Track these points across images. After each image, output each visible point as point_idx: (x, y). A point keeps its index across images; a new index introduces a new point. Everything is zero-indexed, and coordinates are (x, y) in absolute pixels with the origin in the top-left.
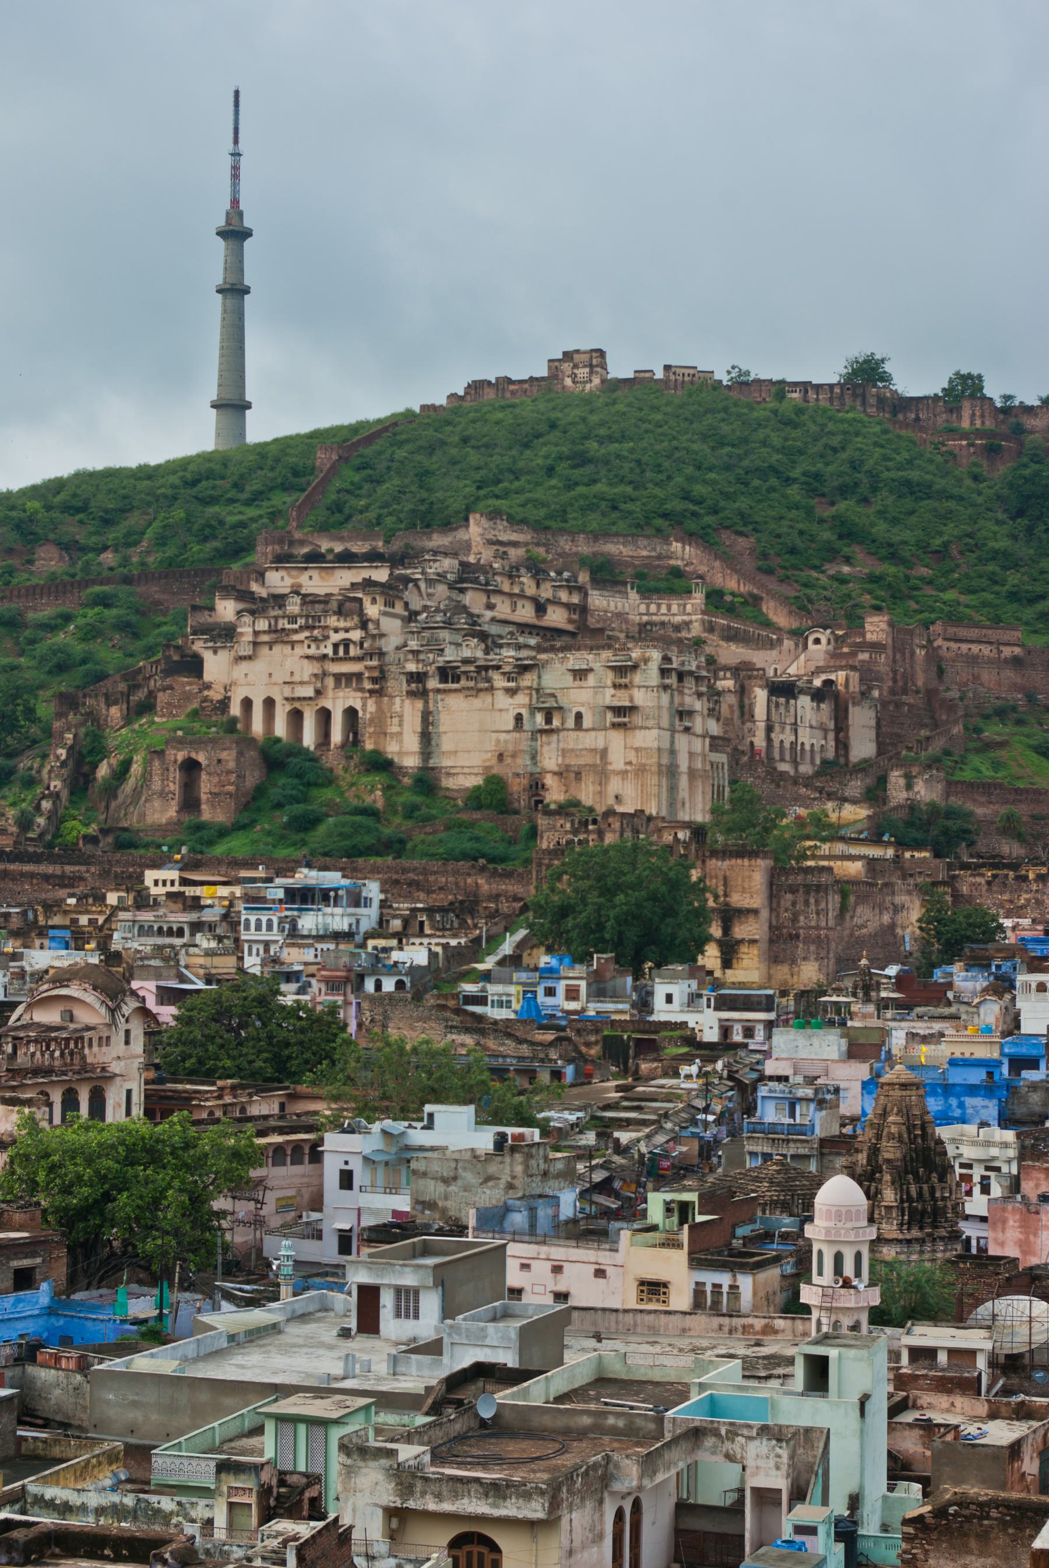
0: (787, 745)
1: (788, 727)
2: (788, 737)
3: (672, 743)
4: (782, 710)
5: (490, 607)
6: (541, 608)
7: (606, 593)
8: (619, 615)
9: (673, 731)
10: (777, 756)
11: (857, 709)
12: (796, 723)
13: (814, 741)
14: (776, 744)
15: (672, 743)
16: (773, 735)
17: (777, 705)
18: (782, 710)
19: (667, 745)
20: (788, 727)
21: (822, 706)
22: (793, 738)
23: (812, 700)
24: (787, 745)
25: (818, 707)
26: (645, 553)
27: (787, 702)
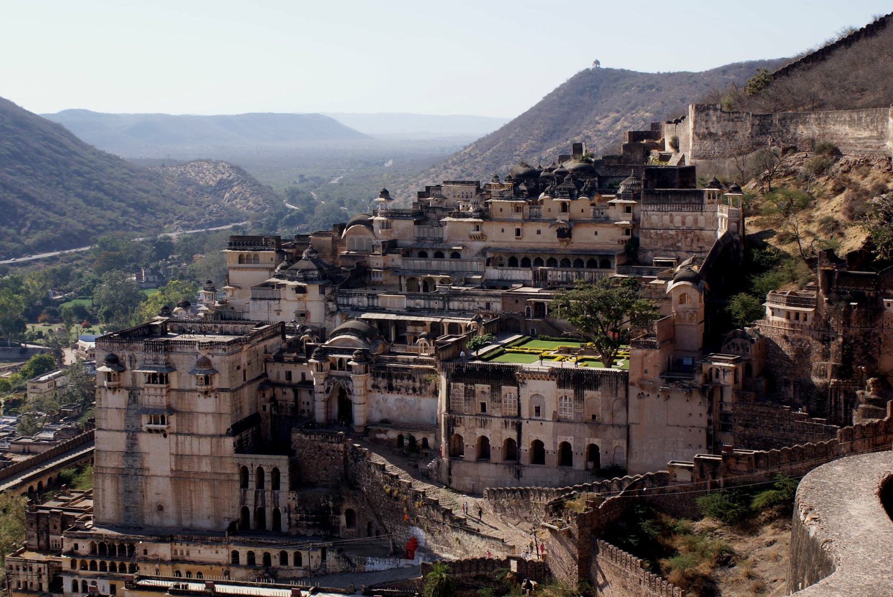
0: (497, 443)
1: (497, 423)
2: (498, 434)
3: (132, 442)
4: (479, 400)
5: (482, 237)
6: (564, 234)
7: (666, 207)
8: (686, 232)
9: (132, 433)
10: (470, 453)
11: (653, 401)
12: (519, 415)
13: (570, 440)
14: (470, 442)
15: (132, 442)
16: (459, 430)
17: (470, 394)
18: (487, 400)
19: (122, 447)
20: (497, 423)
21: (588, 393)
22: (513, 435)
23: (561, 384)
24: (497, 443)
25: (579, 397)
26: (866, 134)
27: (496, 389)
